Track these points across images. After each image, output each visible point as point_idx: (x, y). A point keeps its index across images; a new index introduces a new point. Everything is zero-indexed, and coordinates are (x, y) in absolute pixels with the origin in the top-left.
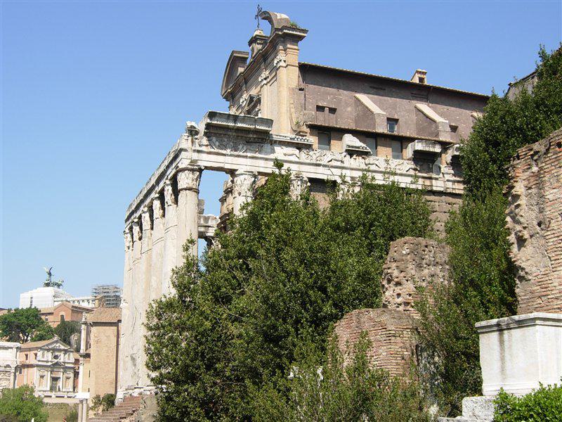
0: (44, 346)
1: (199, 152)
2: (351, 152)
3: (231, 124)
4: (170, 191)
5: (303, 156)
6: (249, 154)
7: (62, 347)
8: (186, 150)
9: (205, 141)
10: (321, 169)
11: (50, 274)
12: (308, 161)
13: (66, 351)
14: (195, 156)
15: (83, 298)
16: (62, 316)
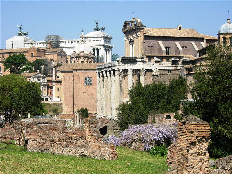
0: (34, 76)
1: (120, 66)
2: (156, 62)
3: (127, 59)
4: (112, 72)
5: (144, 64)
6: (131, 65)
7: (42, 76)
8: (117, 66)
9: (121, 63)
10: (148, 67)
11: (21, 29)
12: (145, 65)
13: (43, 78)
14: (119, 67)
15: (40, 42)
16: (32, 54)
